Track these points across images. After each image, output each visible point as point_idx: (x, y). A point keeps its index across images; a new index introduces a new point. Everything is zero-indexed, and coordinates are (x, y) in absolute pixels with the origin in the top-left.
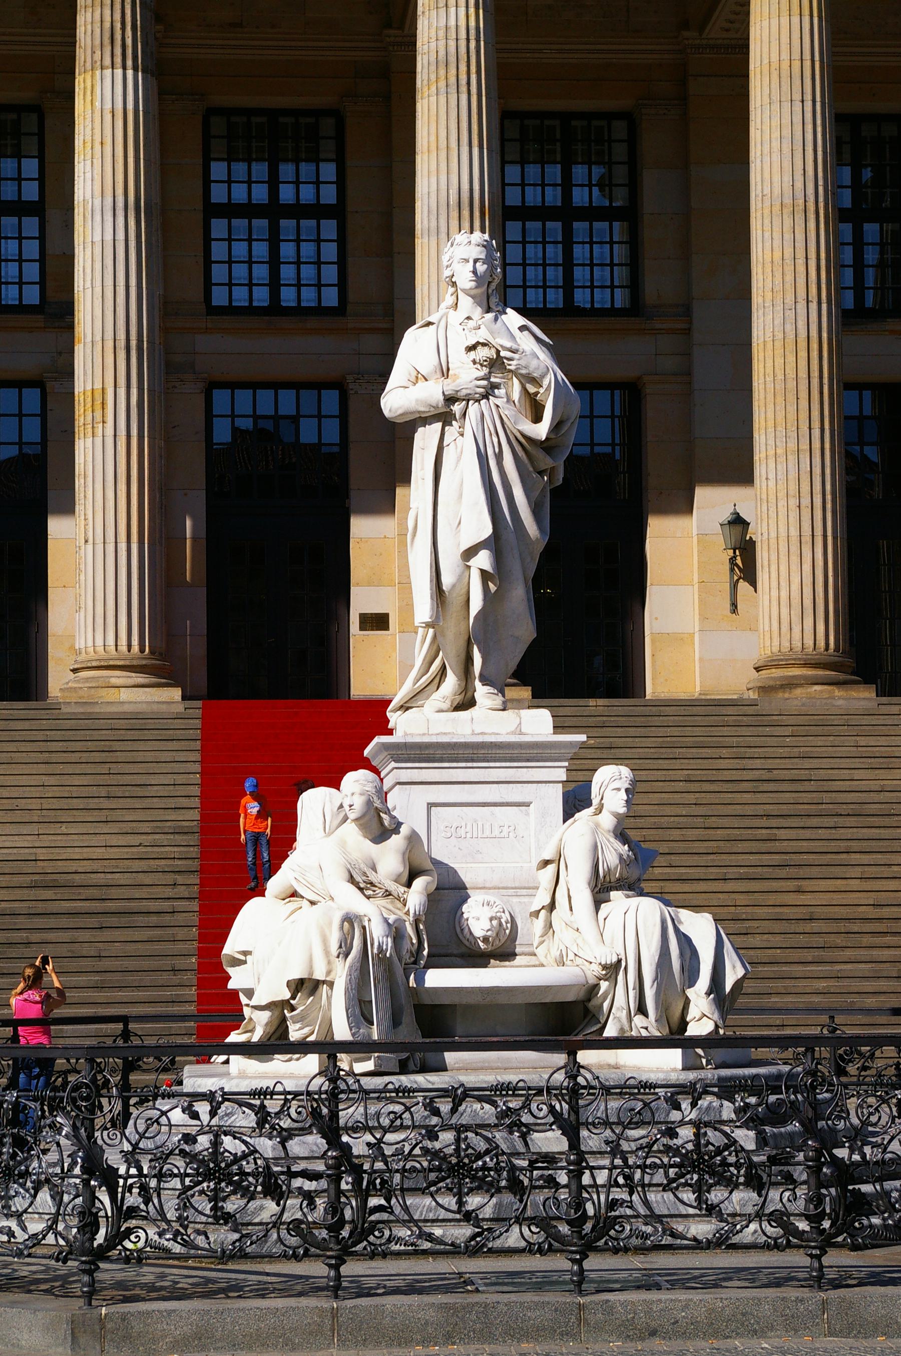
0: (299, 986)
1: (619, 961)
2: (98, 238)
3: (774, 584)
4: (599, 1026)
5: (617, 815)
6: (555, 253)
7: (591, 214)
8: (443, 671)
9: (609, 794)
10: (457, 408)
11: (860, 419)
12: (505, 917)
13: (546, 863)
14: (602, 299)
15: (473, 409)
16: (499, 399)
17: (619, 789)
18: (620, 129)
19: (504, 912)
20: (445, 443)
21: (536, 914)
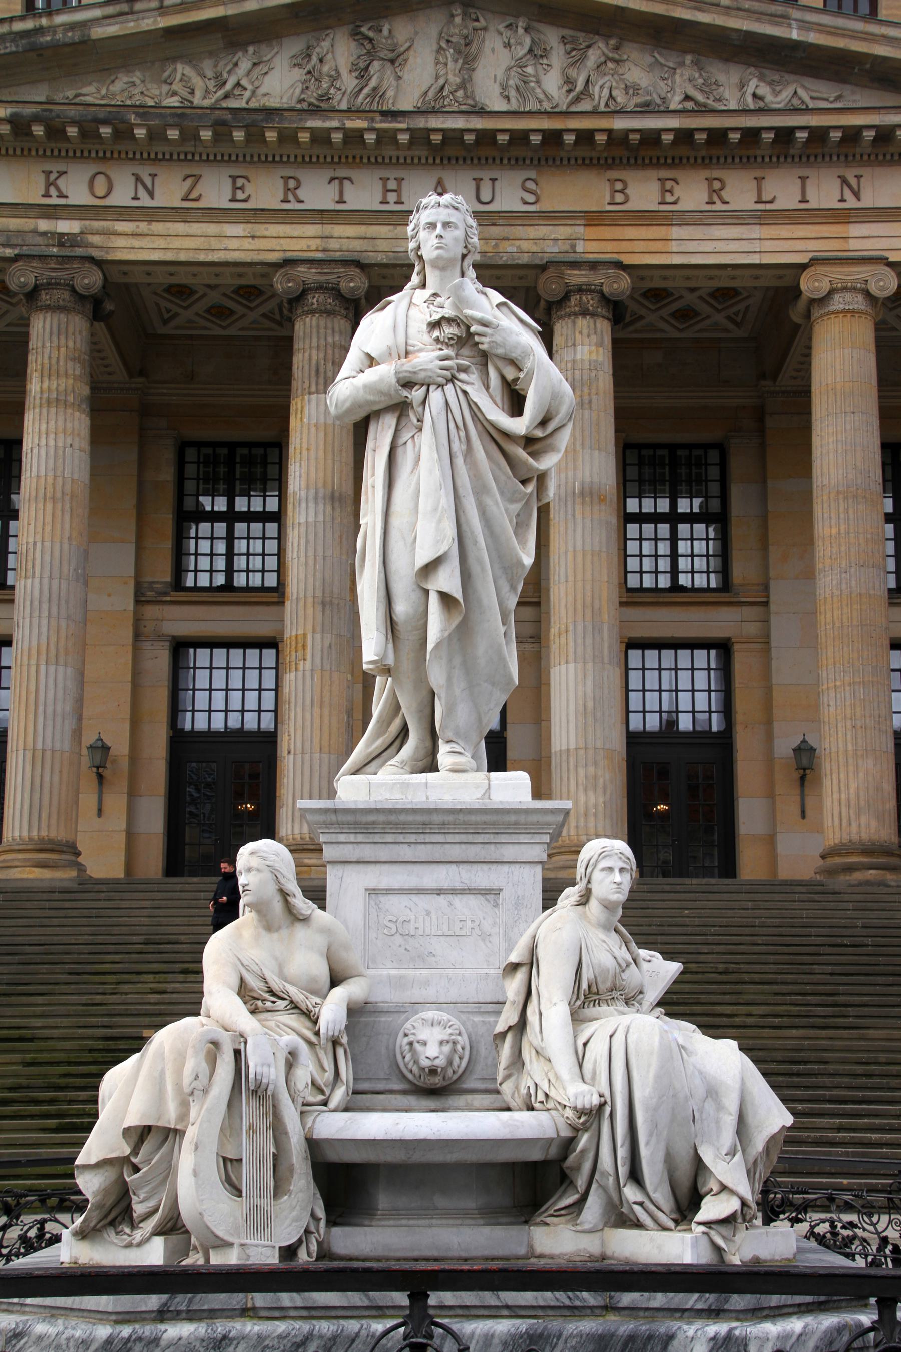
0: (140, 1135)
1: (602, 1105)
2: (303, 520)
3: (836, 788)
4: (576, 1197)
6: (664, 548)
7: (690, 518)
8: (404, 732)
9: (597, 876)
10: (417, 394)
12: (463, 1040)
13: (514, 968)
14: (700, 581)
15: (436, 396)
17: (610, 869)
18: (714, 456)
19: (460, 1034)
20: (401, 441)
21: (503, 1035)
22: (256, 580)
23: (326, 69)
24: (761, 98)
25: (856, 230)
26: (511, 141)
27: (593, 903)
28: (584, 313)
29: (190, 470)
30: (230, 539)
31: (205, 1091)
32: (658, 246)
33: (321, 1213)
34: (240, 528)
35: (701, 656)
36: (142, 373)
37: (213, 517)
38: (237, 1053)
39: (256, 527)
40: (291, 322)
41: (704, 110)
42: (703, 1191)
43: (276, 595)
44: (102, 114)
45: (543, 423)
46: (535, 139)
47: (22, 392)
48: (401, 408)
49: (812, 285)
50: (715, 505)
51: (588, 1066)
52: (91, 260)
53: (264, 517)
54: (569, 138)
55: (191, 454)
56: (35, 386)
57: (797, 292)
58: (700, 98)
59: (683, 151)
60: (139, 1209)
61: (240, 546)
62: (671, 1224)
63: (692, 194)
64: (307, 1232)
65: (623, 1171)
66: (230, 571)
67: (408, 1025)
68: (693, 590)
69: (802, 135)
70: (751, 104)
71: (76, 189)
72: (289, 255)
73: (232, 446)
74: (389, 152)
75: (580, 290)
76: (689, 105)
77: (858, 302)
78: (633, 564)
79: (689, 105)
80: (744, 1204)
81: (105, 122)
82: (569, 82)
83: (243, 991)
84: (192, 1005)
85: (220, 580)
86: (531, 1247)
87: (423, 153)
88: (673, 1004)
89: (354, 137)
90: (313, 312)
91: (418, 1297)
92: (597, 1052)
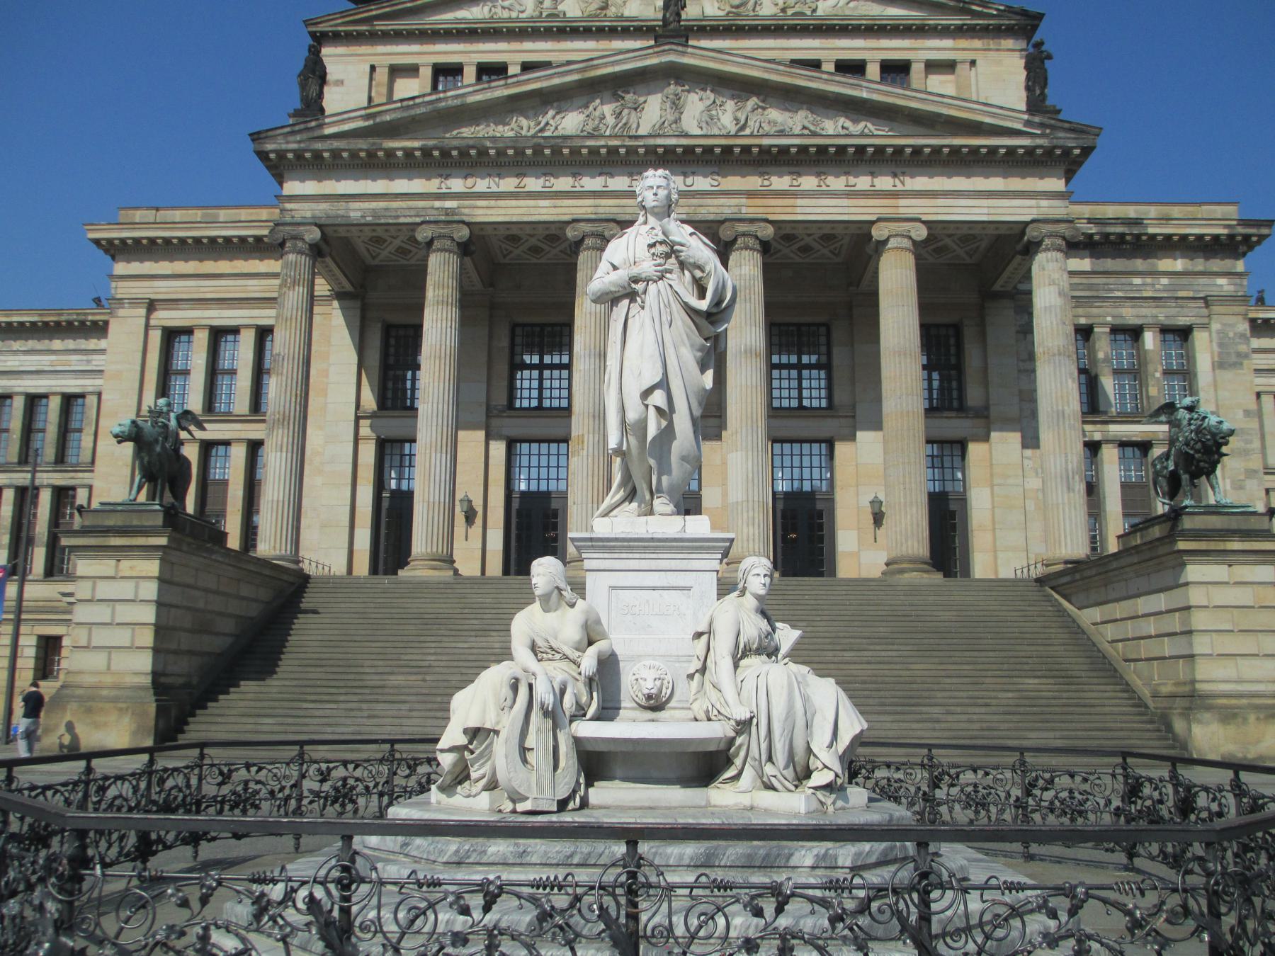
0: (474, 733)
1: (752, 718)
5: (759, 598)
6: (794, 384)
7: (810, 367)
9: (751, 579)
10: (639, 287)
11: (932, 456)
12: (669, 678)
13: (698, 635)
14: (815, 404)
16: (673, 278)
18: (823, 330)
21: (691, 677)
22: (555, 403)
23: (597, 113)
24: (847, 129)
25: (902, 202)
26: (703, 152)
27: (748, 594)
28: (747, 248)
29: (518, 340)
30: (541, 379)
31: (511, 707)
32: (789, 210)
33: (582, 780)
34: (547, 373)
35: (815, 446)
36: (492, 285)
37: (531, 367)
38: (531, 686)
39: (556, 373)
40: (577, 254)
41: (814, 134)
42: (812, 767)
43: (567, 412)
44: (471, 142)
45: (719, 303)
46: (718, 150)
47: (423, 297)
48: (632, 296)
49: (878, 233)
50: (824, 359)
51: (744, 694)
52: (463, 222)
53: (561, 367)
54: (737, 150)
55: (518, 331)
56: (430, 293)
57: (870, 236)
58: (812, 128)
59: (802, 157)
60: (474, 775)
61: (547, 384)
62: (793, 788)
63: (809, 182)
64: (574, 791)
65: (764, 757)
66: (540, 398)
67: (635, 669)
68: (811, 408)
69: (870, 150)
70: (843, 132)
71: (457, 185)
72: (575, 217)
73: (542, 326)
74: (633, 158)
75: (744, 234)
76: (806, 132)
77: (906, 243)
78: (776, 393)
79: (806, 132)
80: (837, 776)
81: (473, 147)
82: (737, 119)
83: (534, 648)
84: (505, 654)
85: (534, 403)
86: (708, 801)
87: (653, 158)
88: (797, 655)
89: (613, 151)
90: (588, 249)
91: (632, 844)
92: (749, 686)
